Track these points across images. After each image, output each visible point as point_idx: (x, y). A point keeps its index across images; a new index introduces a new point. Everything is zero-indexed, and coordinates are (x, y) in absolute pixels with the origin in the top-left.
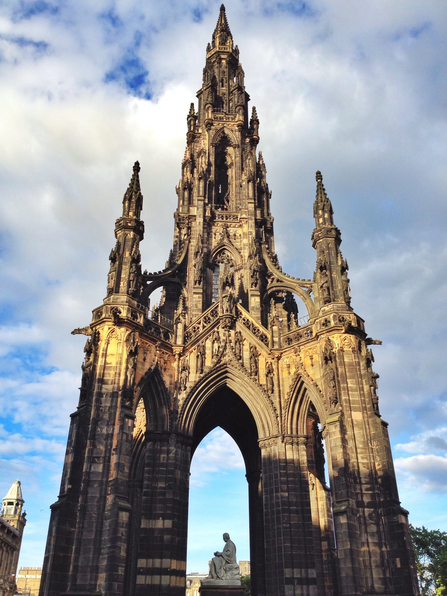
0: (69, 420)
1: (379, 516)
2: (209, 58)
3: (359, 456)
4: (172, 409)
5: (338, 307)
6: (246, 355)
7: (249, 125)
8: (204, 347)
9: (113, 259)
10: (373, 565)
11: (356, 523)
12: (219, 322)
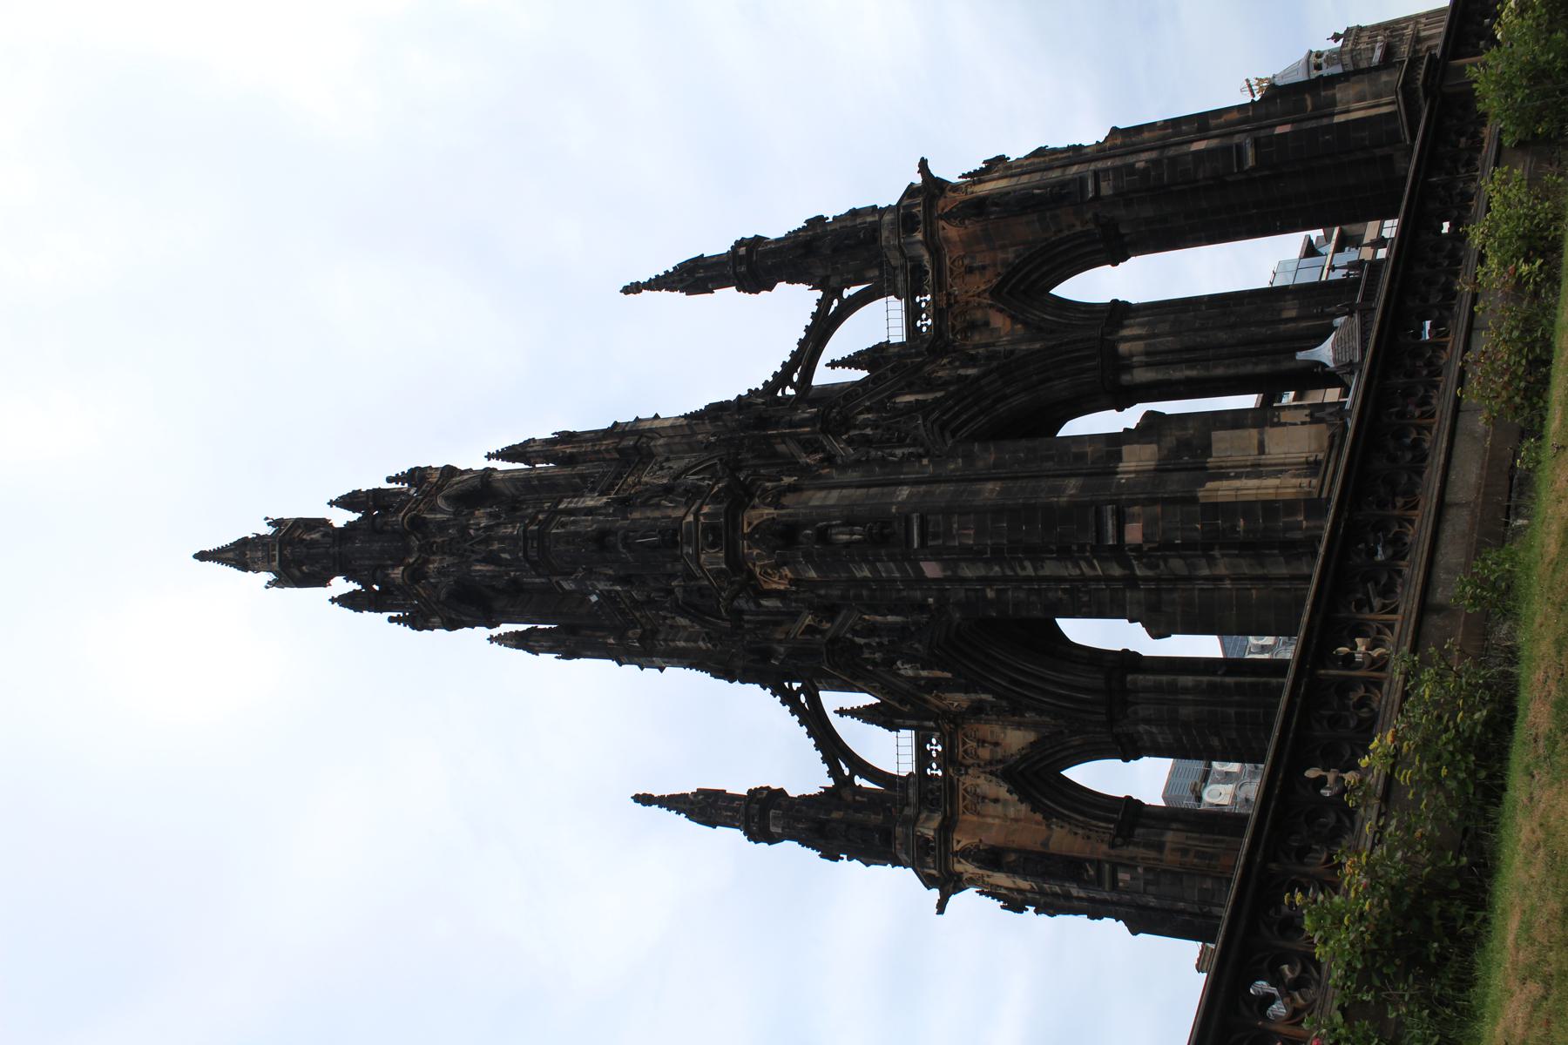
10: (1260, 572)
11: (1176, 595)
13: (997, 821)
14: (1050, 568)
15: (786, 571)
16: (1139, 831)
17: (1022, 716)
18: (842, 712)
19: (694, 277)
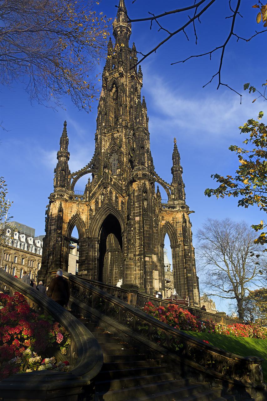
1: (141, 258)
3: (137, 236)
4: (86, 228)
5: (137, 169)
6: (114, 198)
8: (98, 199)
9: (55, 172)
10: (137, 278)
11: (132, 263)
13: (67, 212)
14: (138, 241)
15: (137, 189)
16: (66, 241)
17: (89, 220)
18: (89, 179)
19: (176, 157)
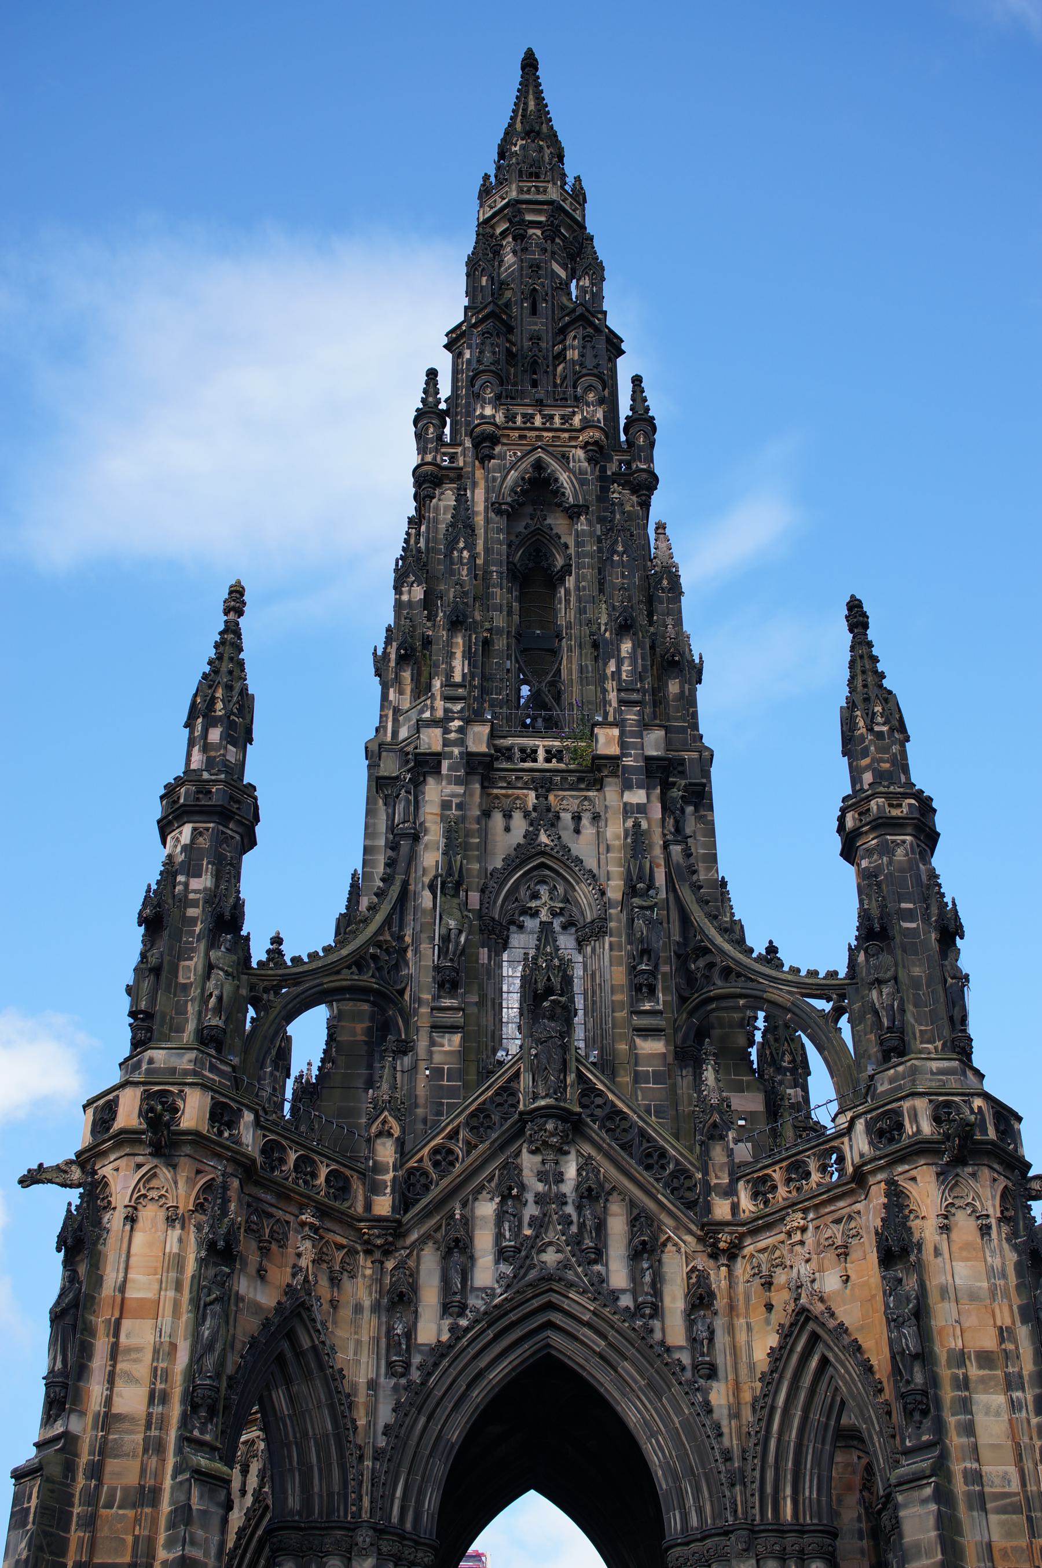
0: (9, 1487)
2: (487, 221)
7: (623, 438)
12: (521, 1132)
